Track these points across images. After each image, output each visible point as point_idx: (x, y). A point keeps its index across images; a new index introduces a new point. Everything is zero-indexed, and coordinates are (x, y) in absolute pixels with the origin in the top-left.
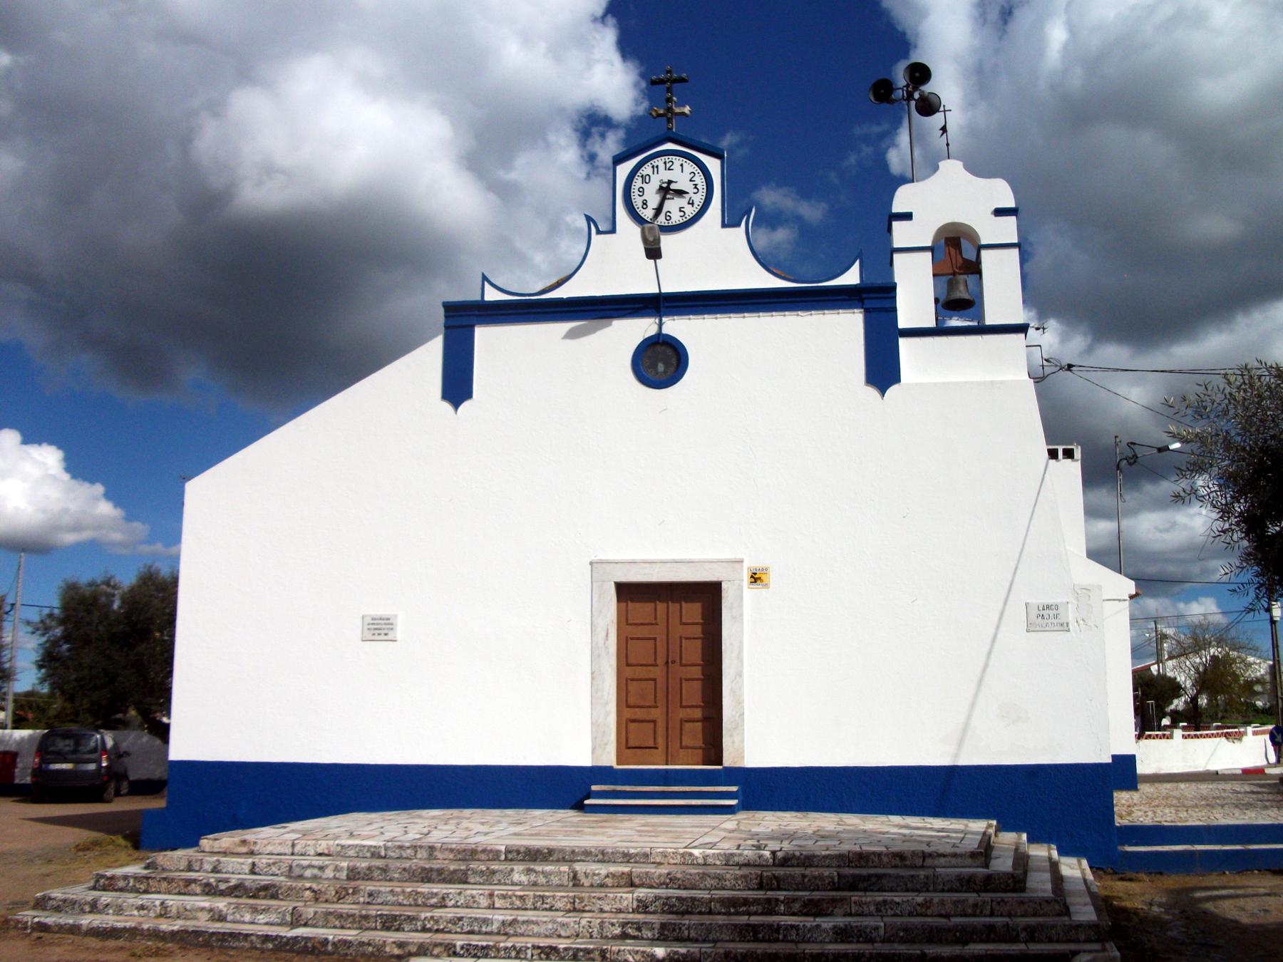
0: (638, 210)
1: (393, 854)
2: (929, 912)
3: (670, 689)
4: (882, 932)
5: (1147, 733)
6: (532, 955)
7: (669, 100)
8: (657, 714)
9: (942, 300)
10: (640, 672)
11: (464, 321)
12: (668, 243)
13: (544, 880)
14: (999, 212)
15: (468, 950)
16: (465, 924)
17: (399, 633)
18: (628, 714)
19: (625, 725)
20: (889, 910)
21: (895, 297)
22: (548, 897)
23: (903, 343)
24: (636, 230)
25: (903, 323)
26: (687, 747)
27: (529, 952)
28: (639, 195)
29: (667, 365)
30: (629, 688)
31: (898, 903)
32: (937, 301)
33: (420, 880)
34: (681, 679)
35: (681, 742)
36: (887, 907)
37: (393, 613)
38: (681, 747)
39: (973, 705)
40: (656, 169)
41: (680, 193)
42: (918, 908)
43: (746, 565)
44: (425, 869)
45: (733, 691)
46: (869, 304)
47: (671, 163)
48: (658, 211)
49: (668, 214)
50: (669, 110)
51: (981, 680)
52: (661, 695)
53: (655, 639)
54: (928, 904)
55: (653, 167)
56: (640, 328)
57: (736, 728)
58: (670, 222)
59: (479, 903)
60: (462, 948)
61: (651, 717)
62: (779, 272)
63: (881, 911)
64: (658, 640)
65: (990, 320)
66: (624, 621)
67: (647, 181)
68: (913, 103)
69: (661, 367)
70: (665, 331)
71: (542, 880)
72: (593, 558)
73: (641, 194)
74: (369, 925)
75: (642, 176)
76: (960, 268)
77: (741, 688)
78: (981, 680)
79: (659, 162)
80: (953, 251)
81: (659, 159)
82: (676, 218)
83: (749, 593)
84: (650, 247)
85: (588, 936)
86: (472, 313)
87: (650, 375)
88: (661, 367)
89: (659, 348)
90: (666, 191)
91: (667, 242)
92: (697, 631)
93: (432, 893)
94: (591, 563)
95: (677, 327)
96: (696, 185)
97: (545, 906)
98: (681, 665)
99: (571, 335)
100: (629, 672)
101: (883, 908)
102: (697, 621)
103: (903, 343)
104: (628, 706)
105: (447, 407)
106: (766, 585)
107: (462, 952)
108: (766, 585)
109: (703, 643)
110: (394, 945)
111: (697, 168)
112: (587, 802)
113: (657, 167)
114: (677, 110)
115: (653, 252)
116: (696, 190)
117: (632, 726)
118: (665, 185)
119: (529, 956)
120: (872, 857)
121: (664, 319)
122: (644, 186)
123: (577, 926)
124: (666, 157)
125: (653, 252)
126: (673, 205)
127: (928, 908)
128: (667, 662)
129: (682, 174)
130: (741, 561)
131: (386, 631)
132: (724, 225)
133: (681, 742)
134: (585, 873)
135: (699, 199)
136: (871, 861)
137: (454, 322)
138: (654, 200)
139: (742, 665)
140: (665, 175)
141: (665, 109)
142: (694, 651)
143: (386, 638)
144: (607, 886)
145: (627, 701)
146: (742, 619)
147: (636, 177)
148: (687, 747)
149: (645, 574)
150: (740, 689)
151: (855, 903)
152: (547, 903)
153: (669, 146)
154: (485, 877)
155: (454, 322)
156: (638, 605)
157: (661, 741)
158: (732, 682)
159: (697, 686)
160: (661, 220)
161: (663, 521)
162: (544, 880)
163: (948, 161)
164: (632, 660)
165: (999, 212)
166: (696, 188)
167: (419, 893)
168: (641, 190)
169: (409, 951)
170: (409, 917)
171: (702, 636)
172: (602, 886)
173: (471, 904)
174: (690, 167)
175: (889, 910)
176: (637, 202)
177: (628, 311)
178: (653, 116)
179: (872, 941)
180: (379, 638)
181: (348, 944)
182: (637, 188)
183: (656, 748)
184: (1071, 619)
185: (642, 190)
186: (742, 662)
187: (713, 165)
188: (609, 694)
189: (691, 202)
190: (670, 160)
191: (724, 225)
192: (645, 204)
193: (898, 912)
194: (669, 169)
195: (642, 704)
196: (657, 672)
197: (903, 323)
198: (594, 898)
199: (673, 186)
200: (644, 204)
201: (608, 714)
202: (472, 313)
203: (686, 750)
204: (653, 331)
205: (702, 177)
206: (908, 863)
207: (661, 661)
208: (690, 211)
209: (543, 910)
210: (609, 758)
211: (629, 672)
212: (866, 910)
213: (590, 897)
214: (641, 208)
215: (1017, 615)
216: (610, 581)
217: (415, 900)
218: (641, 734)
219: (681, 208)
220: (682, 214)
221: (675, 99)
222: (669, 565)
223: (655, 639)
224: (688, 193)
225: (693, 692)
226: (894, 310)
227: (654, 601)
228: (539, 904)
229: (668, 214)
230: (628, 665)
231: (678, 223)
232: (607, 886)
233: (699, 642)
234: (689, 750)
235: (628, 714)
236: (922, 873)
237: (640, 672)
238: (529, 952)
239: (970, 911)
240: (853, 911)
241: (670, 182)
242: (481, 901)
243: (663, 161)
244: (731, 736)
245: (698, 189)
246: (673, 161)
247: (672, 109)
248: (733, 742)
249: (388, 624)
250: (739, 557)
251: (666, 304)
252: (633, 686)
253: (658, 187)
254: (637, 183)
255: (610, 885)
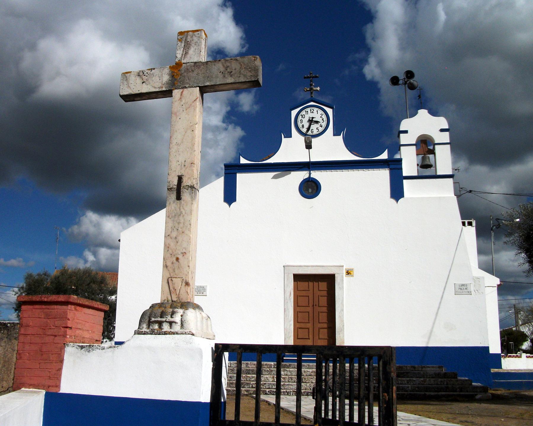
0: (300, 129)
1: (233, 366)
2: (425, 384)
3: (315, 316)
4: (410, 388)
6: (293, 394)
7: (311, 85)
8: (309, 325)
9: (420, 164)
10: (303, 309)
11: (232, 171)
12: (314, 141)
13: (290, 374)
14: (442, 130)
15: (270, 392)
16: (267, 385)
17: (208, 292)
18: (298, 325)
19: (297, 330)
20: (411, 383)
21: (402, 164)
22: (293, 378)
23: (405, 181)
24: (302, 138)
25: (405, 174)
26: (321, 339)
27: (292, 393)
28: (301, 123)
29: (313, 189)
30: (299, 315)
31: (415, 380)
32: (418, 165)
33: (245, 373)
34: (319, 312)
35: (319, 337)
36: (411, 382)
37: (205, 285)
38: (319, 339)
39: (434, 323)
40: (307, 112)
41: (317, 122)
42: (422, 382)
43: (344, 268)
44: (247, 370)
45: (340, 317)
46: (392, 166)
47: (313, 110)
48: (308, 129)
49: (312, 130)
50: (311, 89)
51: (437, 313)
52: (311, 319)
53: (308, 296)
54: (425, 381)
55: (306, 112)
56: (301, 175)
57: (341, 331)
58: (313, 133)
59: (269, 380)
60: (269, 392)
61: (308, 327)
62: (355, 154)
63: (408, 383)
64: (310, 297)
65: (439, 173)
66: (296, 289)
67: (304, 117)
68: (407, 85)
69: (310, 190)
70: (311, 176)
71: (289, 373)
72: (284, 264)
73: (301, 122)
74: (233, 386)
75: (302, 115)
76: (427, 152)
77: (343, 315)
78: (437, 313)
79: (308, 110)
80: (424, 145)
81: (308, 108)
82: (315, 132)
83: (346, 279)
84: (307, 144)
85: (310, 389)
86: (236, 168)
87: (306, 194)
88: (310, 190)
89: (309, 183)
90: (311, 121)
91: (314, 141)
92: (325, 293)
93: (252, 377)
94: (284, 266)
95: (317, 175)
96: (323, 119)
97: (292, 381)
98: (319, 306)
99: (275, 177)
100: (299, 309)
101: (409, 382)
102: (325, 289)
103: (405, 181)
104: (298, 322)
105: (226, 205)
106: (353, 276)
107: (268, 393)
108: (353, 276)
109: (327, 298)
110: (245, 391)
111: (323, 112)
112: (284, 358)
113: (307, 111)
114: (315, 89)
115: (309, 146)
116: (323, 121)
117: (299, 330)
118: (311, 119)
119: (292, 394)
120: (404, 367)
121: (311, 172)
122: (303, 119)
123: (306, 386)
124: (311, 108)
125: (309, 146)
126: (314, 127)
127: (425, 382)
128: (313, 305)
129: (317, 114)
130: (343, 266)
131: (203, 292)
132: (334, 135)
133: (319, 337)
134: (304, 371)
135: (324, 124)
136: (403, 368)
137: (228, 171)
138: (306, 125)
139: (343, 307)
140: (311, 115)
141: (310, 88)
142: (324, 301)
143: (203, 294)
144: (312, 376)
145: (297, 320)
146: (343, 288)
147: (299, 116)
148: (321, 339)
149: (305, 271)
150: (343, 316)
151: (400, 380)
152: (293, 380)
153: (312, 103)
154: (269, 373)
155: (228, 171)
156: (301, 283)
157: (311, 337)
158: (340, 313)
159: (325, 314)
160: (310, 133)
161: (312, 250)
162: (290, 374)
163: (452, 183)
164: (299, 304)
165: (442, 130)
166: (323, 120)
167: (248, 376)
168: (301, 120)
169: (250, 393)
170: (247, 383)
171: (327, 295)
172: (310, 375)
173: (266, 380)
174: (320, 112)
175: (411, 383)
176: (300, 125)
177: (297, 169)
178: (305, 91)
179: (406, 391)
180: (200, 294)
181: (229, 391)
182: (300, 120)
183: (309, 339)
184: (472, 290)
185: (301, 121)
186: (343, 305)
187: (330, 111)
188: (291, 317)
189: (321, 126)
190: (313, 109)
191: (334, 135)
192: (303, 126)
193: (415, 383)
194: (312, 113)
195: (303, 321)
196: (310, 309)
197: (405, 174)
198: (309, 378)
199: (314, 120)
200: (303, 126)
201: (291, 325)
202: (236, 168)
203: (321, 340)
204: (307, 176)
205: (325, 116)
206: (416, 369)
207: (311, 305)
208: (321, 129)
209: (291, 382)
210: (291, 342)
211: (299, 309)
212: (404, 383)
213: (308, 378)
214: (301, 128)
215: (451, 289)
216: (291, 273)
217: (246, 379)
218: (303, 333)
219: (317, 128)
220: (318, 130)
221: (313, 84)
222: (314, 267)
223: (308, 296)
224: (320, 122)
225: (324, 317)
226: (401, 169)
227: (308, 281)
228: (290, 380)
229: (312, 130)
230: (298, 306)
231: (316, 134)
232: (312, 376)
233: (326, 297)
234: (322, 340)
235: (298, 325)
236: (422, 372)
237: (303, 309)
238: (292, 393)
239: (439, 383)
240: (399, 383)
241: (313, 118)
242: (270, 379)
243: (310, 109)
244: (339, 334)
245: (324, 121)
246: (314, 109)
247: (313, 88)
248: (340, 337)
249: (204, 289)
250: (342, 264)
251: (312, 166)
252: (300, 314)
253: (308, 120)
254: (300, 118)
255: (313, 375)
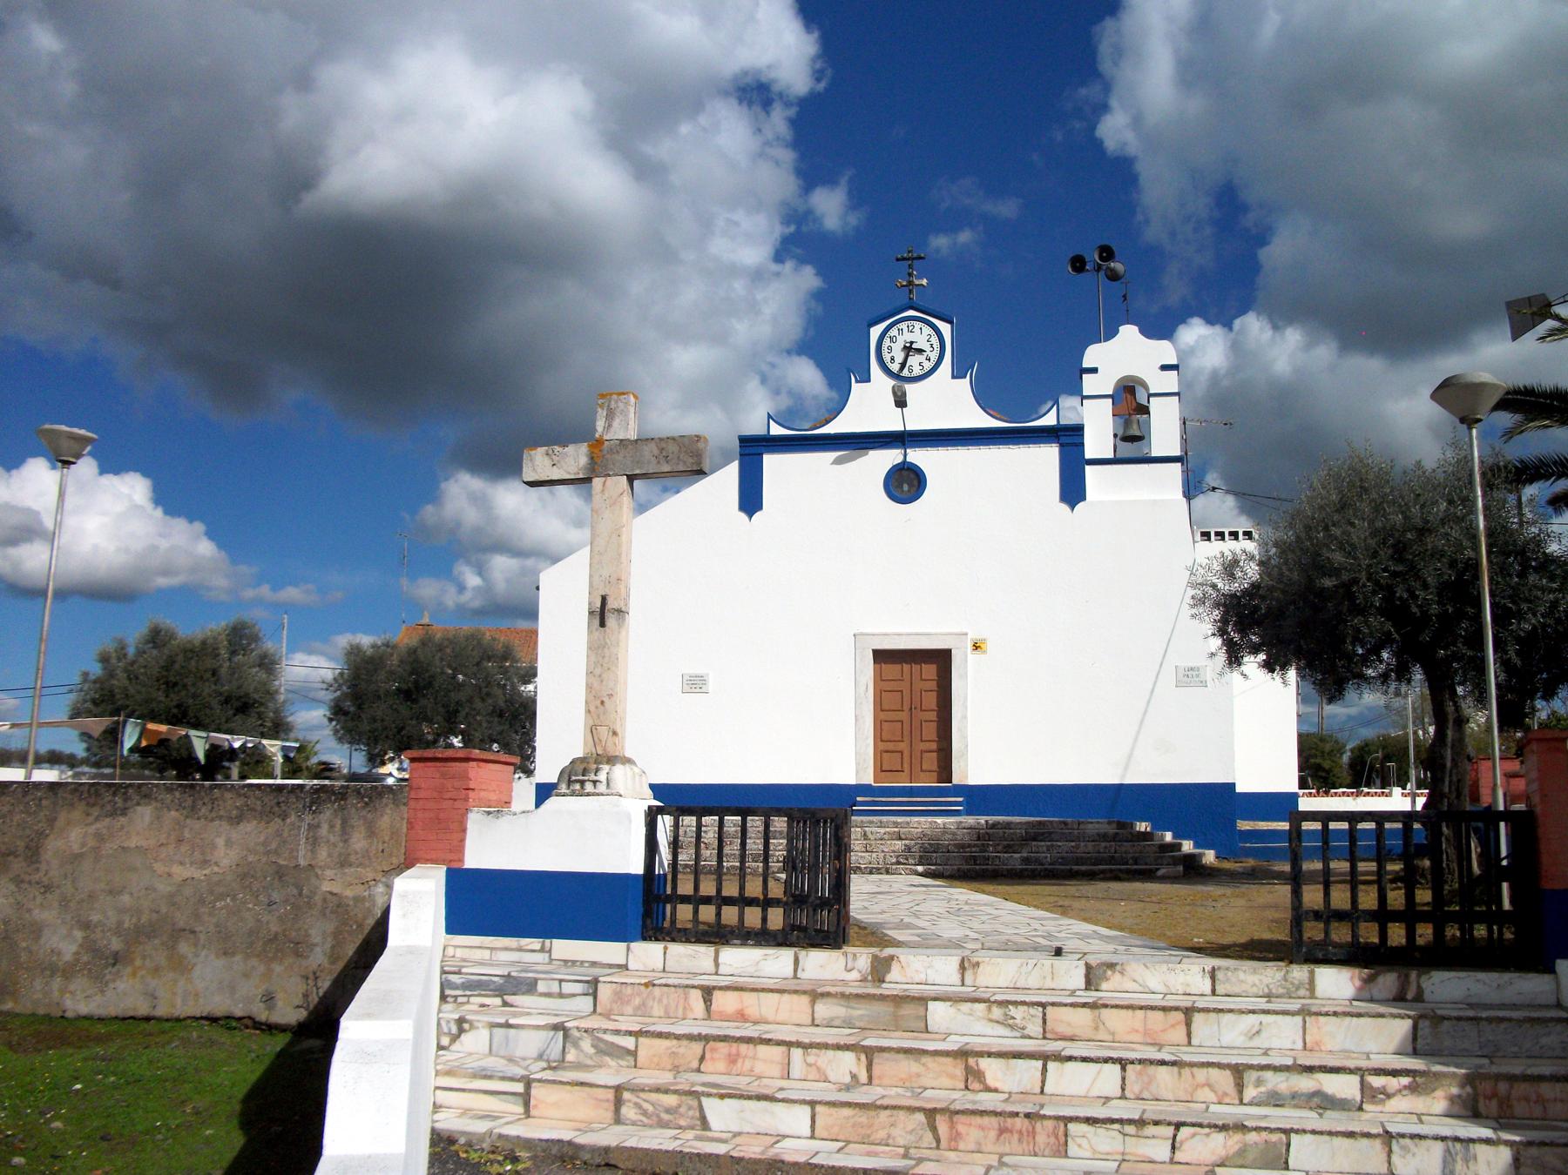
5: (1333, 791)
7: (910, 275)
8: (903, 746)
9: (1120, 433)
10: (891, 715)
14: (1164, 368)
18: (882, 746)
19: (880, 755)
21: (1083, 435)
23: (1088, 468)
25: (1088, 455)
29: (910, 485)
32: (1115, 436)
38: (922, 771)
39: (1136, 740)
41: (920, 351)
43: (969, 637)
46: (1064, 440)
48: (903, 365)
50: (910, 283)
51: (1142, 722)
52: (906, 733)
53: (902, 691)
56: (891, 457)
65: (1154, 454)
66: (879, 678)
69: (906, 487)
70: (908, 460)
76: (1134, 410)
77: (966, 727)
78: (1142, 722)
79: (903, 325)
80: (1129, 396)
82: (917, 371)
83: (972, 657)
88: (906, 487)
90: (909, 349)
92: (933, 685)
99: (837, 462)
100: (883, 716)
103: (1088, 468)
105: (743, 516)
106: (985, 652)
108: (985, 652)
114: (917, 282)
115: (901, 402)
118: (908, 345)
121: (908, 451)
122: (892, 345)
125: (901, 402)
126: (914, 360)
129: (920, 335)
130: (966, 634)
132: (954, 377)
135: (934, 356)
138: (900, 357)
140: (908, 337)
142: (931, 700)
157: (906, 766)
159: (934, 725)
160: (905, 373)
165: (1164, 368)
174: (927, 330)
176: (887, 358)
184: (1209, 679)
185: (890, 348)
186: (966, 708)
187: (945, 328)
191: (954, 377)
196: (904, 716)
197: (1088, 455)
199: (914, 346)
204: (899, 459)
207: (906, 707)
208: (928, 366)
210: (868, 778)
211: (883, 716)
215: (1169, 677)
218: (892, 761)
223: (902, 691)
225: (931, 731)
226: (1082, 444)
233: (935, 694)
235: (882, 746)
237: (891, 715)
241: (912, 343)
250: (964, 631)
252: (885, 725)
254: (886, 343)
